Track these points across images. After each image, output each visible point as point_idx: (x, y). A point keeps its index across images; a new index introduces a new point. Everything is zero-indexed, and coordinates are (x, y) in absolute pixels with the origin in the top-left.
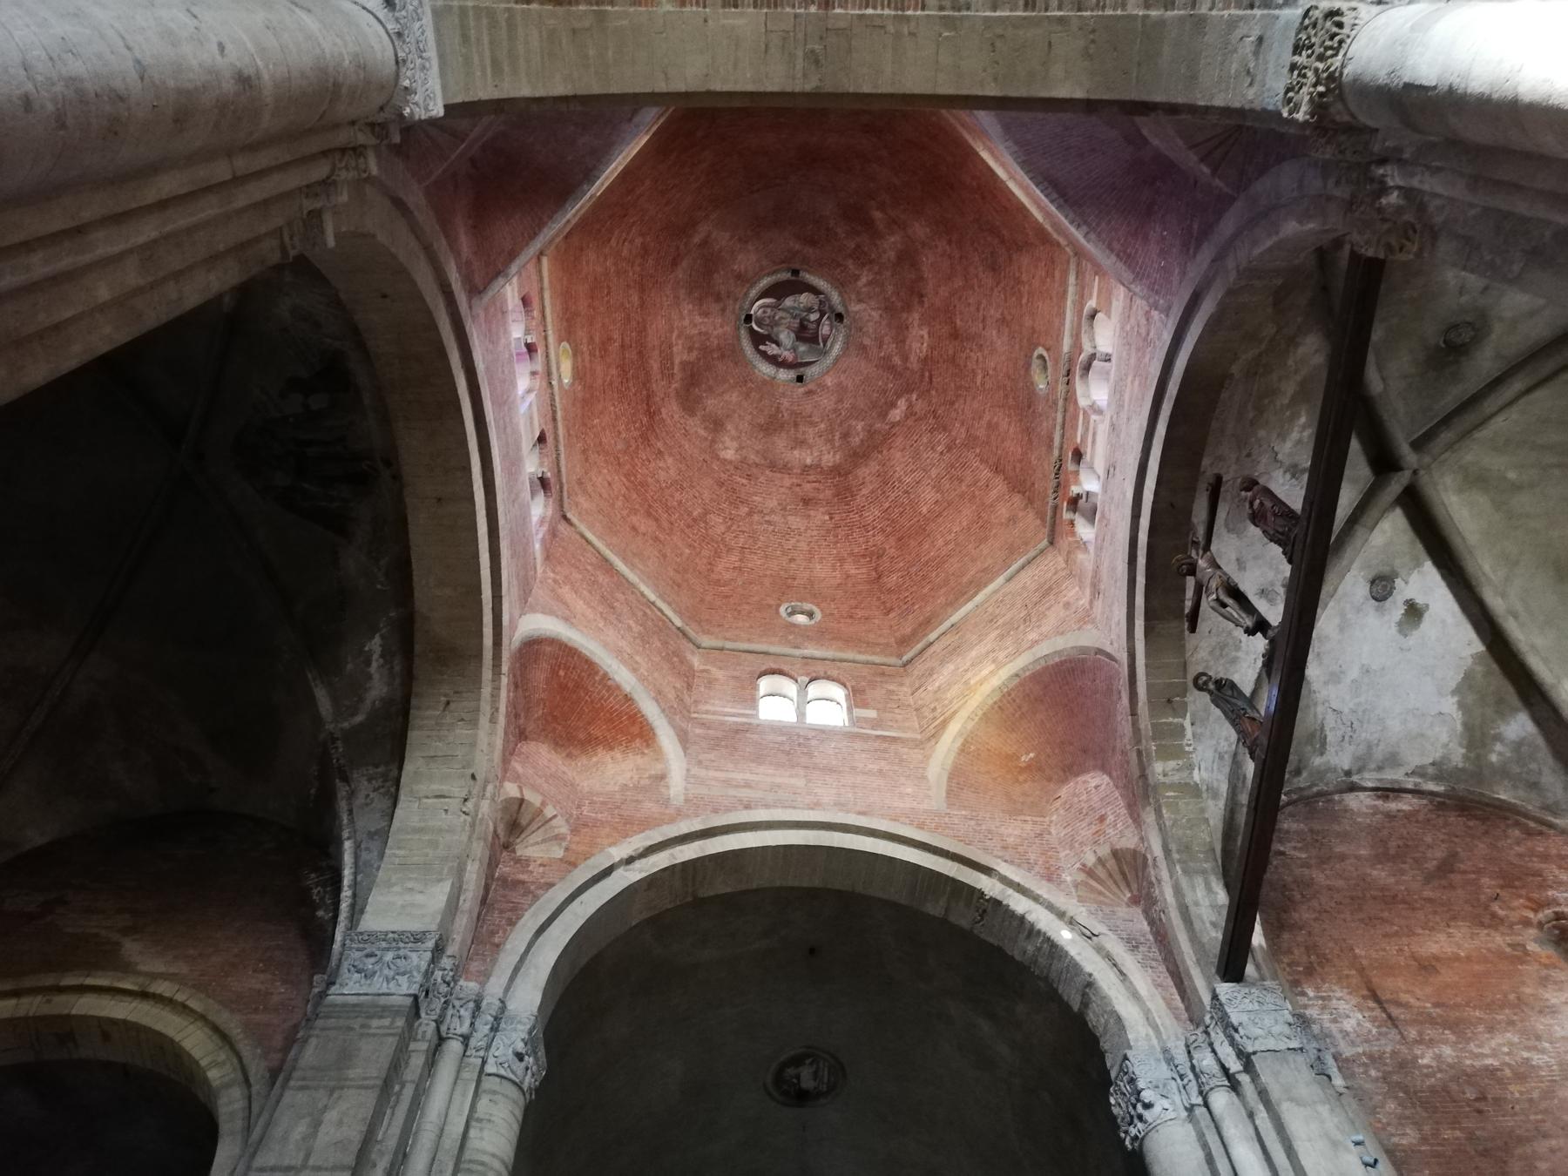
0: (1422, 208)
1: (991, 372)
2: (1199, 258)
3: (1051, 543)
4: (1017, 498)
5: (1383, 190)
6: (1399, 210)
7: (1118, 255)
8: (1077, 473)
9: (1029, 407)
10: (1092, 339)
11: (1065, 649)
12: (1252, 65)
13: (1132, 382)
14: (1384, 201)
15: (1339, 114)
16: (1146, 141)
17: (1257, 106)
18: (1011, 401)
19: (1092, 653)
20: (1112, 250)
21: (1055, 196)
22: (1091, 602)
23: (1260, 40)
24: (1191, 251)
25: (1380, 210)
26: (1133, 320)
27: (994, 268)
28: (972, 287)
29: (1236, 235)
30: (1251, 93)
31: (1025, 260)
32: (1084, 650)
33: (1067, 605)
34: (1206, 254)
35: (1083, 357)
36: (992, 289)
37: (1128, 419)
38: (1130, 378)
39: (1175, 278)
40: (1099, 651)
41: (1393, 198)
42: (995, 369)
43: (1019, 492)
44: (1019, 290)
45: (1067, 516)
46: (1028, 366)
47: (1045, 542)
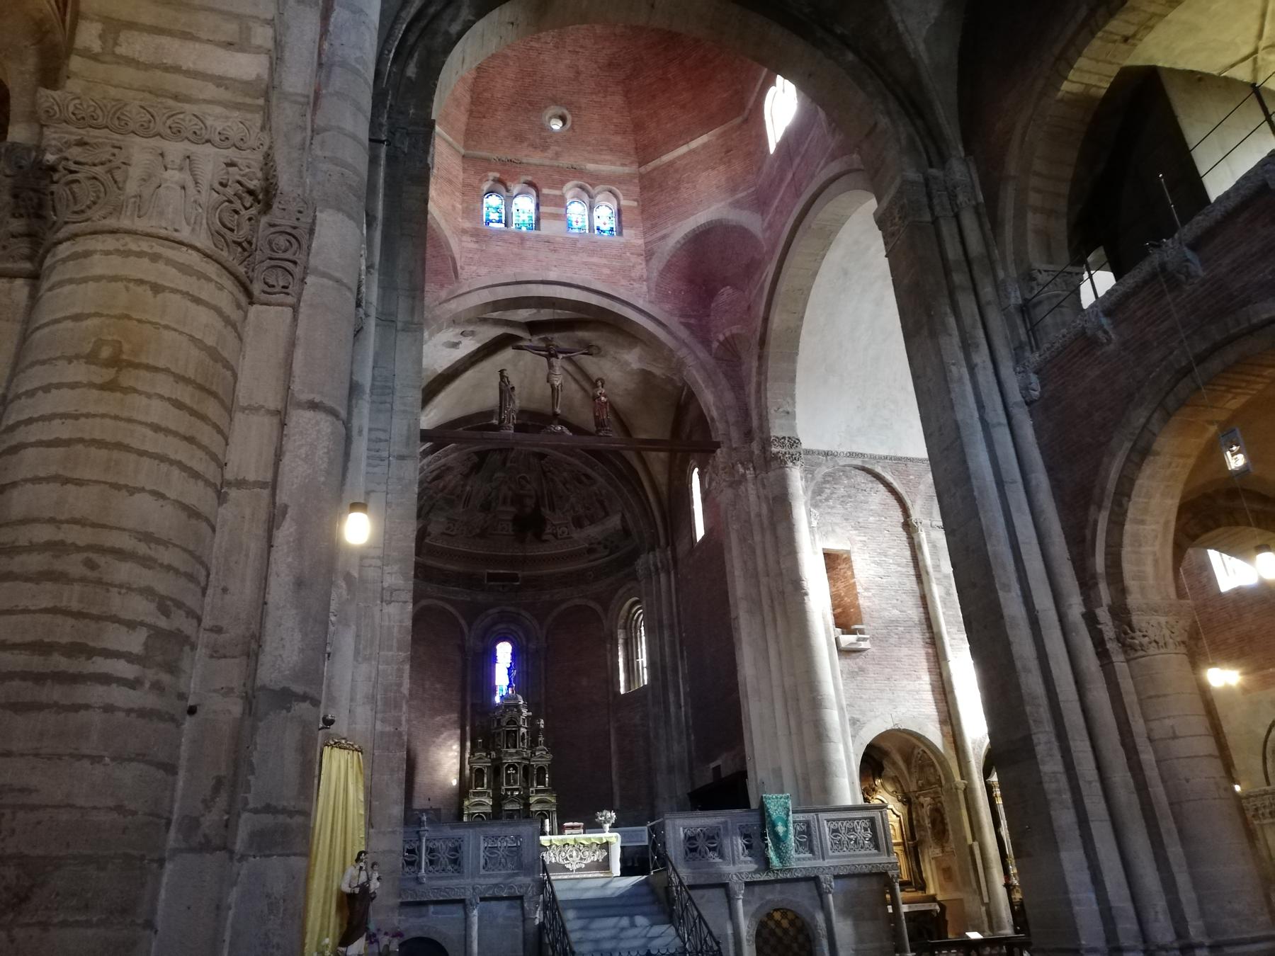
0: (740, 482)
1: (541, 57)
2: (682, 327)
3: (463, 156)
4: (467, 99)
5: (746, 468)
6: (738, 472)
7: (669, 261)
8: (519, 183)
9: (530, 103)
10: (598, 193)
11: (443, 231)
12: (781, 410)
13: (605, 266)
14: (739, 465)
15: (774, 464)
16: (724, 286)
17: (769, 417)
18: (527, 80)
19: (449, 253)
20: (672, 257)
21: (701, 230)
22: (464, 231)
23: (788, 413)
24: (683, 320)
25: (736, 464)
26: (634, 259)
27: (611, 65)
28: (596, 43)
29: (697, 358)
30: (772, 411)
31: (619, 100)
32: (449, 248)
33: (454, 207)
34: (683, 333)
35: (589, 187)
36: (596, 62)
37: (586, 263)
38: (604, 261)
39: (667, 307)
40: (453, 259)
41: (741, 470)
42: (544, 61)
43: (472, 97)
44: (599, 92)
45: (492, 175)
46: (555, 101)
47: (463, 151)
